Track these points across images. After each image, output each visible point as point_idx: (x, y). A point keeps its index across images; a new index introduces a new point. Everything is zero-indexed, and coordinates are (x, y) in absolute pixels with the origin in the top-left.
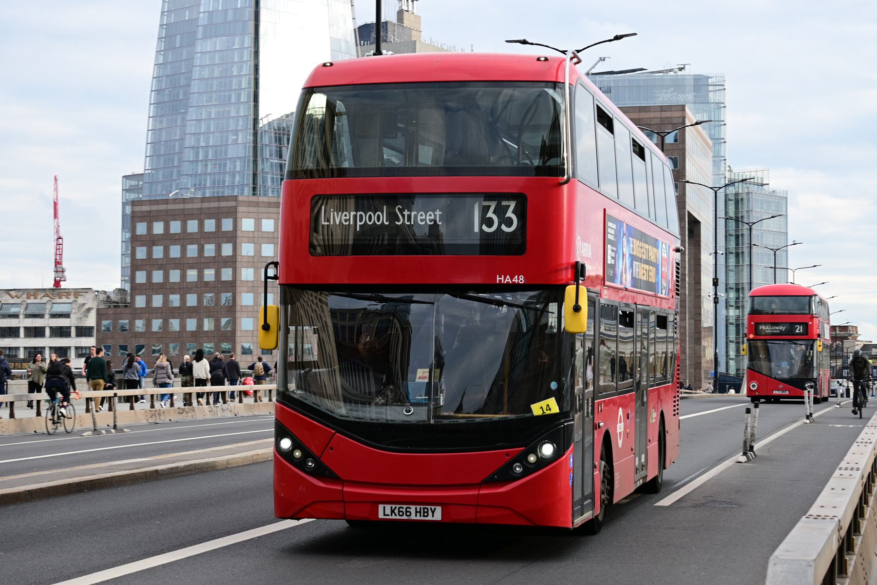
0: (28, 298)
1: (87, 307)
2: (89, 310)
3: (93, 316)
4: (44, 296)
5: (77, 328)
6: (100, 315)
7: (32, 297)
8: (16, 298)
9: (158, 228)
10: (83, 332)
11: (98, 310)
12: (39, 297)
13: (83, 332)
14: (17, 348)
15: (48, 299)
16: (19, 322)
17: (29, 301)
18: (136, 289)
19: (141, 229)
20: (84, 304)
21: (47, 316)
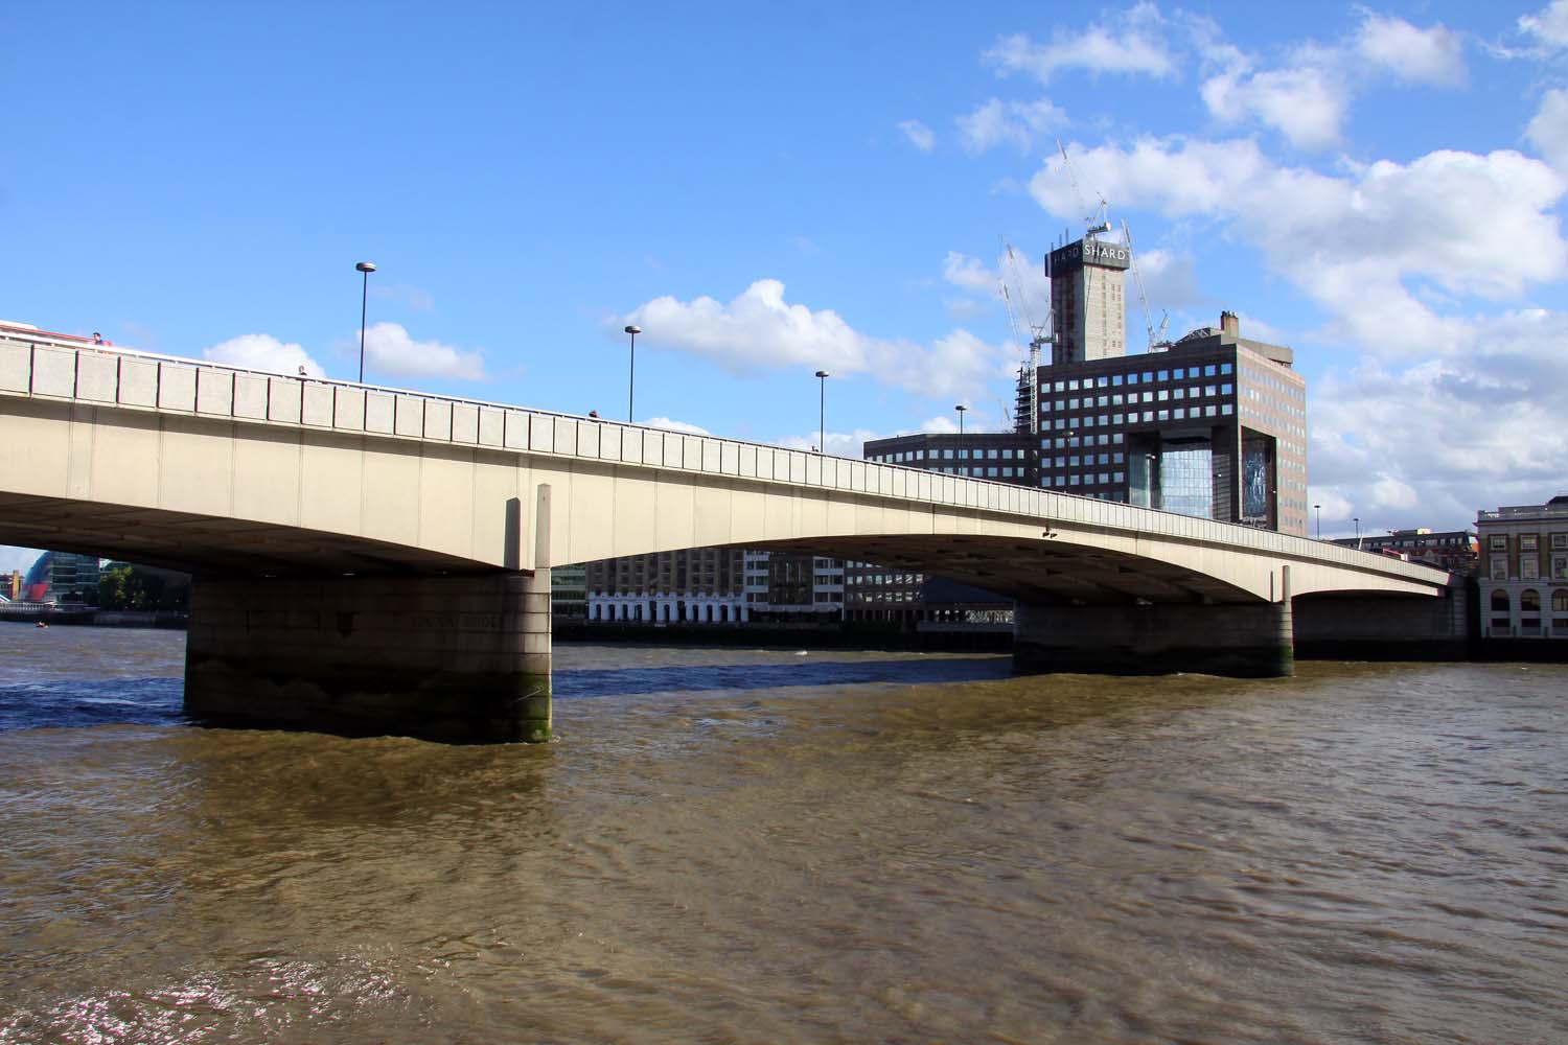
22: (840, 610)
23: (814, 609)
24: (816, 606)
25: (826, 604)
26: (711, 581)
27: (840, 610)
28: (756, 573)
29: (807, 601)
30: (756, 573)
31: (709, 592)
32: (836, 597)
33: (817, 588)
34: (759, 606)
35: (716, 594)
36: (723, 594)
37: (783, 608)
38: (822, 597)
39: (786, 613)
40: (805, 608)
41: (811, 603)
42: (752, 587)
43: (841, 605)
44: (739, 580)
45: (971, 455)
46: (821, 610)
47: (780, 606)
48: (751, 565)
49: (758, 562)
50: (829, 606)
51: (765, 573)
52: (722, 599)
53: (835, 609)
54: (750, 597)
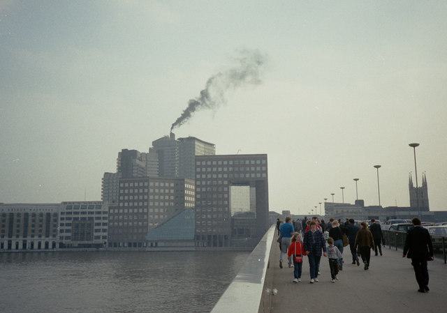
10: (105, 213)
19: (122, 185)
22: (105, 243)
24: (95, 241)
26: (40, 231)
28: (65, 228)
30: (65, 228)
31: (40, 236)
32: (104, 237)
33: (95, 234)
35: (43, 237)
36: (47, 236)
38: (98, 237)
40: (90, 242)
43: (106, 241)
44: (55, 231)
48: (62, 225)
50: (101, 241)
51: (70, 228)
52: (47, 238)
54: (61, 238)
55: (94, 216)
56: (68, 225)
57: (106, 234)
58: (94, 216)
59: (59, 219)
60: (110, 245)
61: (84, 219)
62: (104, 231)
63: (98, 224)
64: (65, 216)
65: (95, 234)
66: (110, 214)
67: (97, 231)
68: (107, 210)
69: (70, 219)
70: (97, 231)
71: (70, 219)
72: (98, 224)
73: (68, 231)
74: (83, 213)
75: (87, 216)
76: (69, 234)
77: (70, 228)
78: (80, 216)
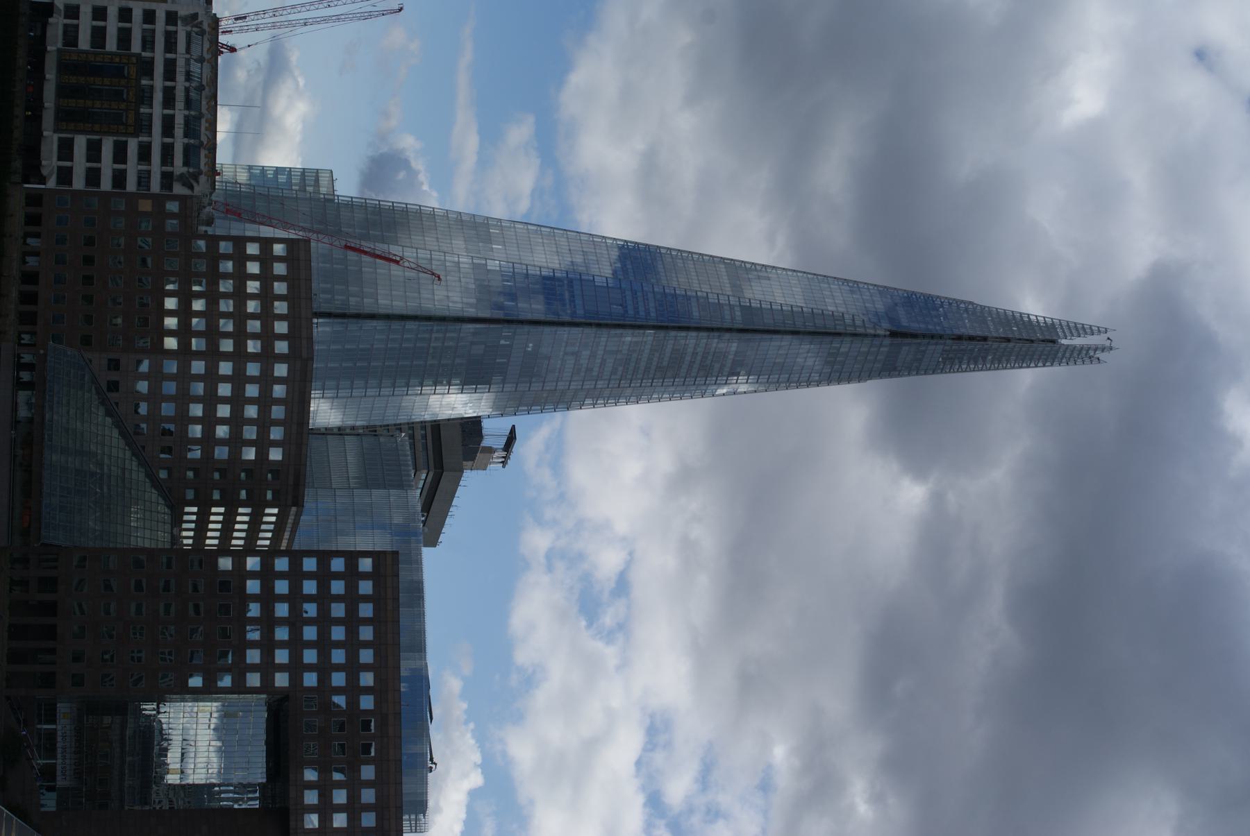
0: (206, 121)
1: (195, 184)
2: (191, 188)
3: (185, 191)
4: (208, 138)
5: (172, 173)
6: (182, 199)
7: (207, 125)
8: (207, 107)
9: (280, 269)
11: (191, 197)
12: (208, 133)
13: (167, 179)
14: (151, 106)
15: (205, 143)
16: (180, 110)
17: (203, 121)
18: (213, 240)
20: (198, 182)
21: (186, 140)
22: (43, 180)
23: (45, 133)
24: (51, 140)
25: (55, 158)
27: (43, 180)
29: (65, 118)
32: (65, 176)
33: (80, 143)
34: (57, 23)
37: (51, 75)
38: (66, 150)
39: (42, 79)
41: (55, 132)
42: (90, 15)
43: (52, 183)
45: (277, 423)
46: (44, 148)
47: (54, 72)
49: (129, 31)
50: (50, 161)
51: (111, 45)
53: (45, 172)
55: (157, 140)
56: (124, 37)
57: (79, 183)
58: (157, 140)
59: (148, 6)
60: (34, 199)
61: (145, 97)
62: (93, 177)
63: (120, 154)
64: (160, 26)
65: (80, 143)
66: (159, 201)
67: (94, 152)
68: (178, 189)
69: (148, 42)
70: (94, 152)
71: (148, 42)
72: (120, 154)
73: (99, 36)
74: (169, 100)
75: (157, 111)
76: (84, 42)
77: (111, 45)
78: (158, 82)
